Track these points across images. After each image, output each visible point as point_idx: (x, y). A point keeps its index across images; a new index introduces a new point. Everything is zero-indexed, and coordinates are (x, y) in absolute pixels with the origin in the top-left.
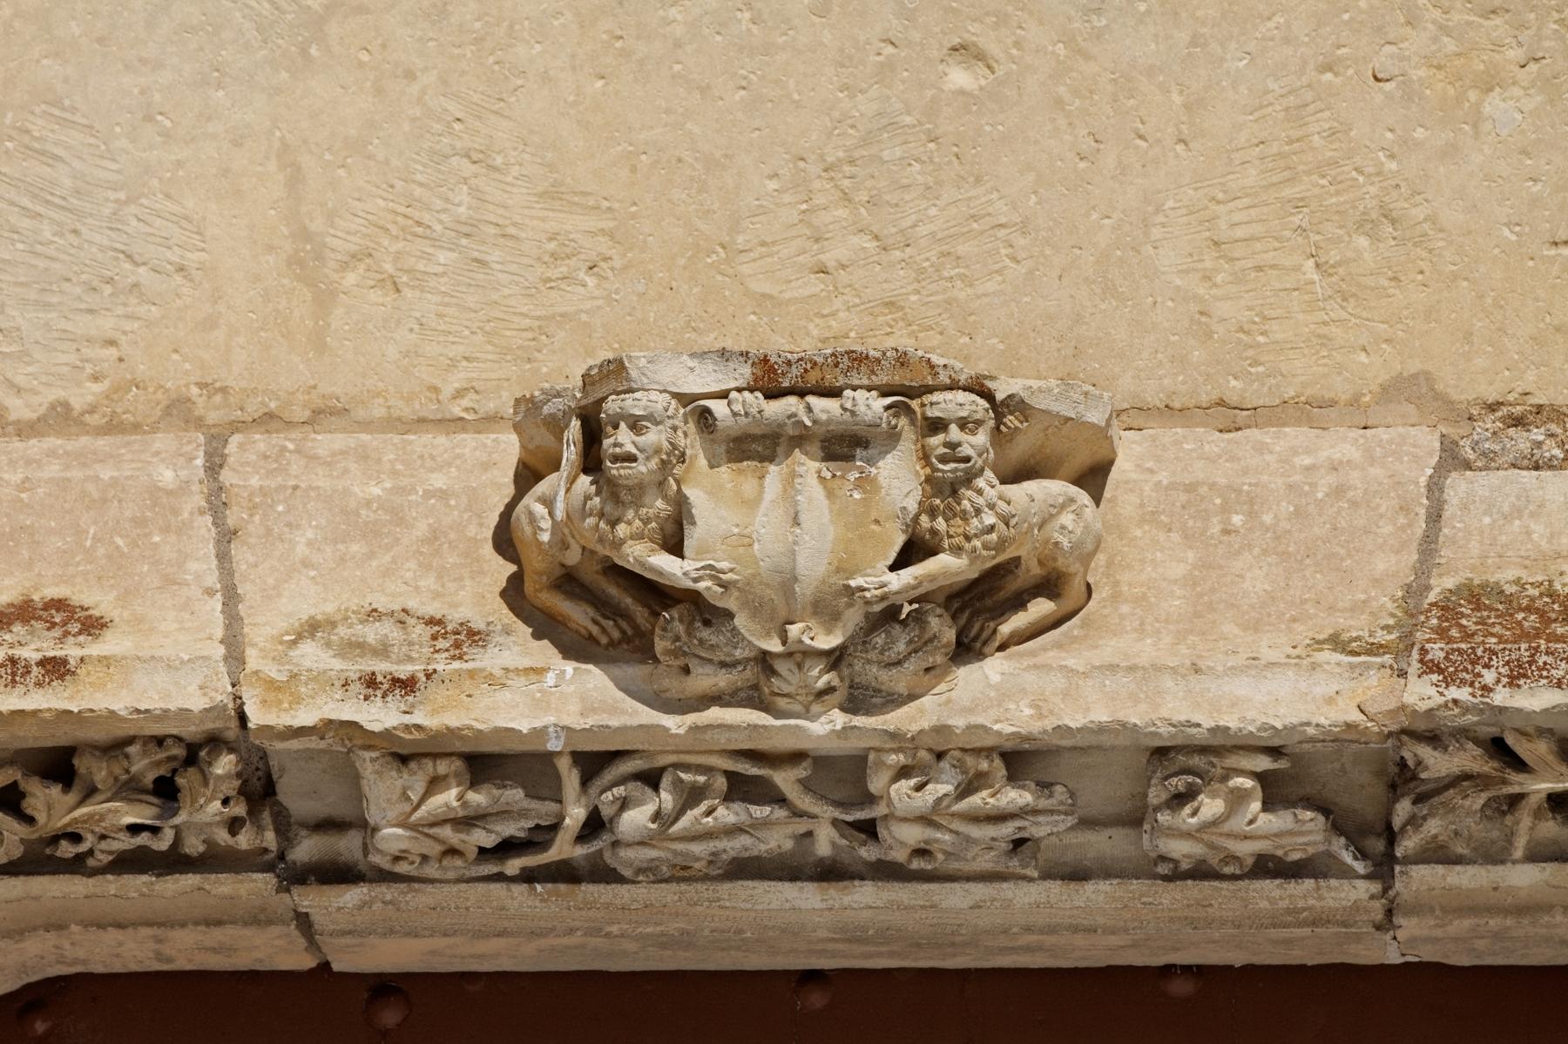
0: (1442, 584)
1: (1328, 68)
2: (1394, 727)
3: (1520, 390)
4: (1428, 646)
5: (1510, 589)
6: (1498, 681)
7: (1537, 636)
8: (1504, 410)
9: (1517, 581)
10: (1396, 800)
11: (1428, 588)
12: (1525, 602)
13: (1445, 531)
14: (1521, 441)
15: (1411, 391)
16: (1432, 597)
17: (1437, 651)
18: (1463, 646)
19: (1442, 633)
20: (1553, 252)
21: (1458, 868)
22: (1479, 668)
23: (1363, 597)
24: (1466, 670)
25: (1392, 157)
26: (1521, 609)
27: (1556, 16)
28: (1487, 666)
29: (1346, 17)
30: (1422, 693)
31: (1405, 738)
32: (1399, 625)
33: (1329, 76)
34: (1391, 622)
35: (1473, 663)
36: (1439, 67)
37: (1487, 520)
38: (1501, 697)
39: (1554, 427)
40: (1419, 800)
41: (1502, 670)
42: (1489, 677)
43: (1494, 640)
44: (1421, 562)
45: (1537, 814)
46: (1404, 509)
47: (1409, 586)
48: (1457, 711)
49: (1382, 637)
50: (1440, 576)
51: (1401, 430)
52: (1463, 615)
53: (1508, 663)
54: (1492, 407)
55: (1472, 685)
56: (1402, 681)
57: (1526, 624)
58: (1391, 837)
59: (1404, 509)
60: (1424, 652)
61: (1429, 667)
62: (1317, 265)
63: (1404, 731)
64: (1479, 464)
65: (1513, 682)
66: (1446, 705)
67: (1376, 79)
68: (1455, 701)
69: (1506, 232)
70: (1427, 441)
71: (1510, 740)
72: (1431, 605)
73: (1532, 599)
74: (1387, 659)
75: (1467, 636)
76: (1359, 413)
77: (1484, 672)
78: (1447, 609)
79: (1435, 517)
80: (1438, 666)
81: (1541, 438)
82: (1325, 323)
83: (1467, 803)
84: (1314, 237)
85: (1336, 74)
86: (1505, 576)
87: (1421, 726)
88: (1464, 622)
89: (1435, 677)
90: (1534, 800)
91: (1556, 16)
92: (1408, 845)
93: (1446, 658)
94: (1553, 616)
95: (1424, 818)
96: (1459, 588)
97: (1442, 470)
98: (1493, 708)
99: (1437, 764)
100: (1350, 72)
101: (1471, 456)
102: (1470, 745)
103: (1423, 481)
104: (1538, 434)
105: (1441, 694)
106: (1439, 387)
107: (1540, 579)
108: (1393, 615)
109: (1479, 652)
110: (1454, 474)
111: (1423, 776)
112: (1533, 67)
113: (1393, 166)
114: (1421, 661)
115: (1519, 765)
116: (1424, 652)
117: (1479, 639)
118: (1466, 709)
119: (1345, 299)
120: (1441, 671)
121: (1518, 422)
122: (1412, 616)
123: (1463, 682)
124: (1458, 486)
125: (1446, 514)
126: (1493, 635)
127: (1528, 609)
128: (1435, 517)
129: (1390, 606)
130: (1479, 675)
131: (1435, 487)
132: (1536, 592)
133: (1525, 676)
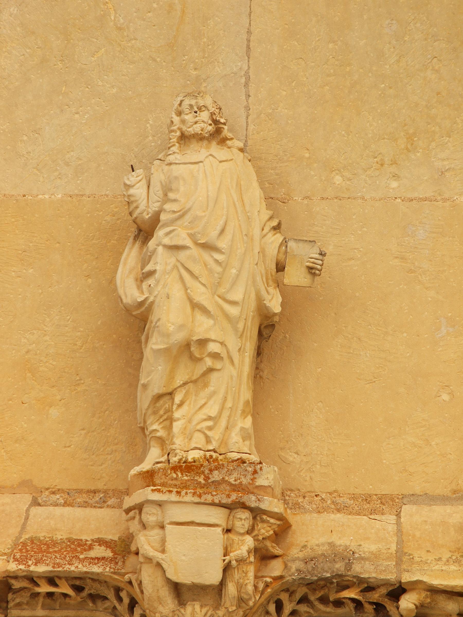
0: (25, 536)
1: (10, 400)
2: (5, 576)
3: (54, 485)
4: (16, 554)
5: (42, 538)
6: (32, 564)
7: (44, 552)
8: (50, 490)
9: (44, 536)
10: (9, 593)
11: (21, 538)
12: (45, 542)
13: (29, 522)
14: (54, 498)
15: (25, 485)
16: (21, 541)
17: (18, 556)
18: (25, 554)
19: (21, 550)
20: (65, 449)
21: (24, 611)
22: (28, 560)
23: (4, 540)
24: (24, 561)
25: (25, 423)
26: (43, 544)
27: (69, 388)
28: (30, 560)
29: (16, 387)
30: (13, 567)
31: (8, 578)
32: (12, 547)
33: (10, 402)
34: (10, 547)
35: (27, 559)
36: (39, 400)
37: (40, 520)
38: (32, 568)
39: (62, 495)
40: (13, 594)
41: (34, 561)
42: (30, 563)
43: (33, 553)
44: (21, 530)
45: (44, 597)
46: (19, 516)
47: (17, 537)
48: (21, 571)
49: (7, 551)
50: (25, 534)
51: (23, 495)
52: (28, 546)
53: (35, 559)
54: (47, 489)
55: (25, 565)
56: (8, 563)
57: (43, 548)
58: (7, 602)
59: (19, 516)
60: (14, 556)
61: (15, 560)
62: (5, 451)
63: (8, 576)
64: (42, 504)
65: (36, 564)
66: (18, 570)
67: (23, 403)
68: (20, 569)
69: (53, 444)
70: (28, 498)
71: (35, 579)
72: (21, 542)
73: (47, 541)
74: (5, 557)
75: (27, 551)
76: (13, 490)
77: (29, 561)
78: (24, 544)
79: (27, 518)
80: (18, 559)
81: (59, 497)
82: (6, 466)
83: (26, 594)
84: (4, 444)
85: (13, 402)
86: (41, 535)
87: (11, 575)
88: (28, 547)
89: (17, 562)
90: (43, 595)
91: (69, 388)
92: (11, 605)
93: (20, 557)
94: (51, 546)
95: (15, 598)
96: (29, 538)
97: (31, 506)
98: (30, 571)
99: (16, 585)
100: (16, 401)
101: (40, 501)
102: (25, 580)
103: (25, 509)
104: (58, 496)
105: (17, 567)
106: (34, 483)
107: (50, 536)
108: (11, 545)
109: (29, 556)
110: (33, 507)
111: (13, 588)
112: (63, 401)
113: (26, 426)
114: (13, 558)
115: (38, 585)
116: (14, 556)
117: (29, 552)
118: (24, 571)
119: (11, 460)
120: (18, 561)
121: (53, 493)
122: (15, 545)
123: (23, 564)
124: (35, 510)
125: (30, 518)
126: (33, 551)
127: (45, 544)
128: (27, 518)
129: (11, 542)
130: (28, 562)
131: (28, 510)
132: (48, 539)
133: (39, 563)
